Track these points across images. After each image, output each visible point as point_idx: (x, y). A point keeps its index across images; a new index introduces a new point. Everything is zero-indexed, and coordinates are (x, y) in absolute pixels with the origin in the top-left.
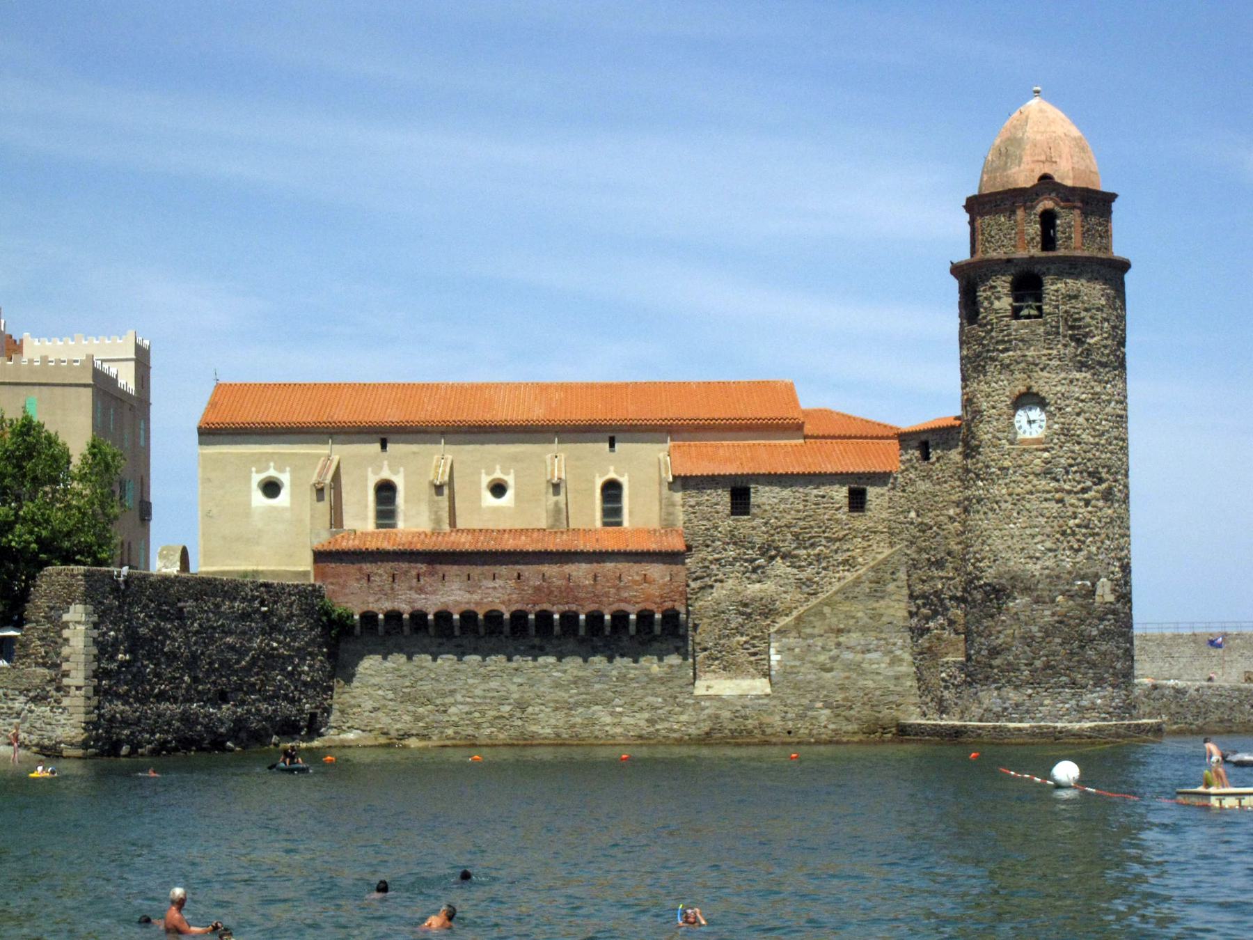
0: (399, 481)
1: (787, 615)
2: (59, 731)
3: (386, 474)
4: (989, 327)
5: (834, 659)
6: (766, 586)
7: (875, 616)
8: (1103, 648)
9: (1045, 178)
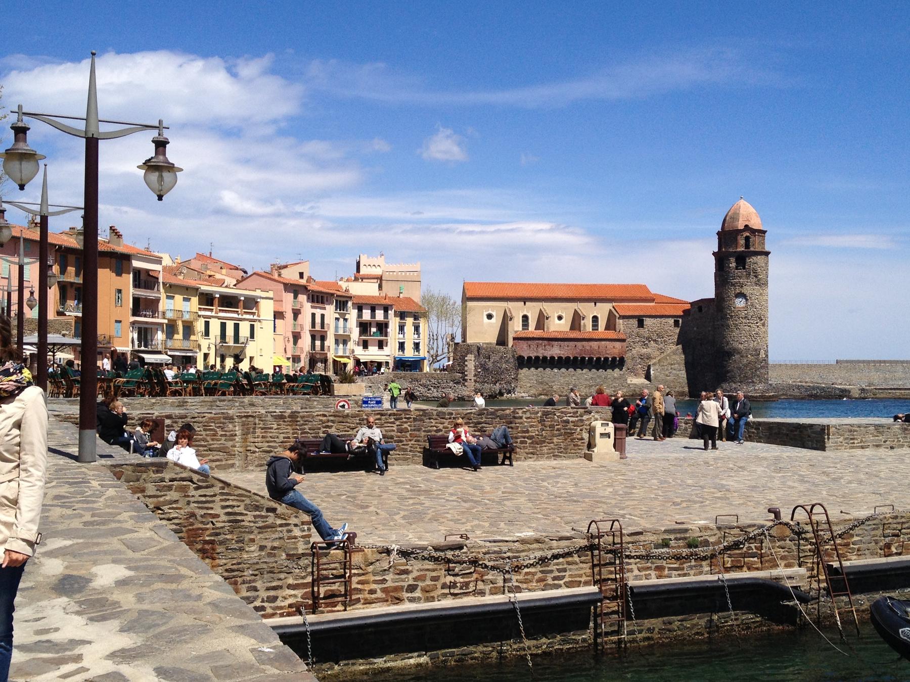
0: (529, 315)
2: (464, 392)
3: (525, 313)
5: (670, 373)
8: (762, 371)
9: (746, 226)
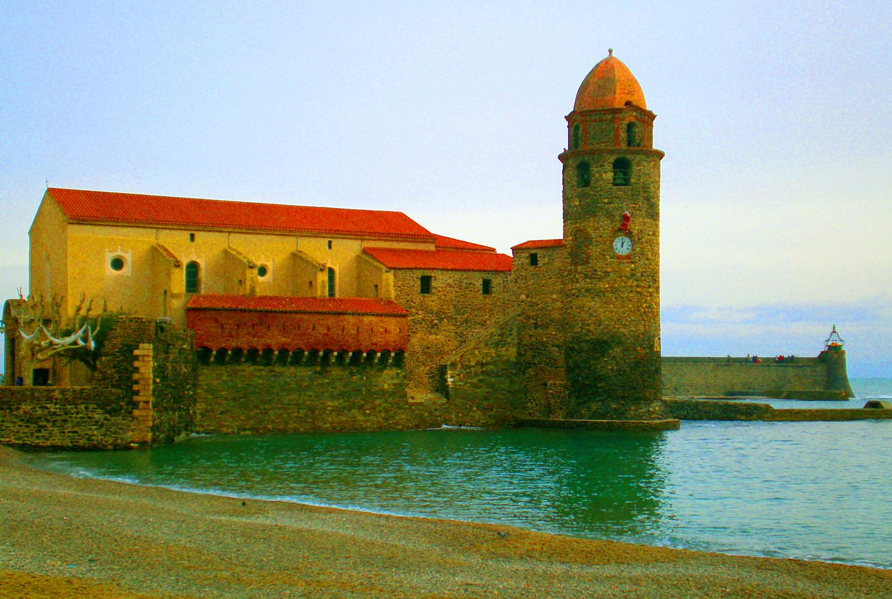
1: (449, 354)
4: (599, 189)
5: (480, 381)
6: (438, 337)
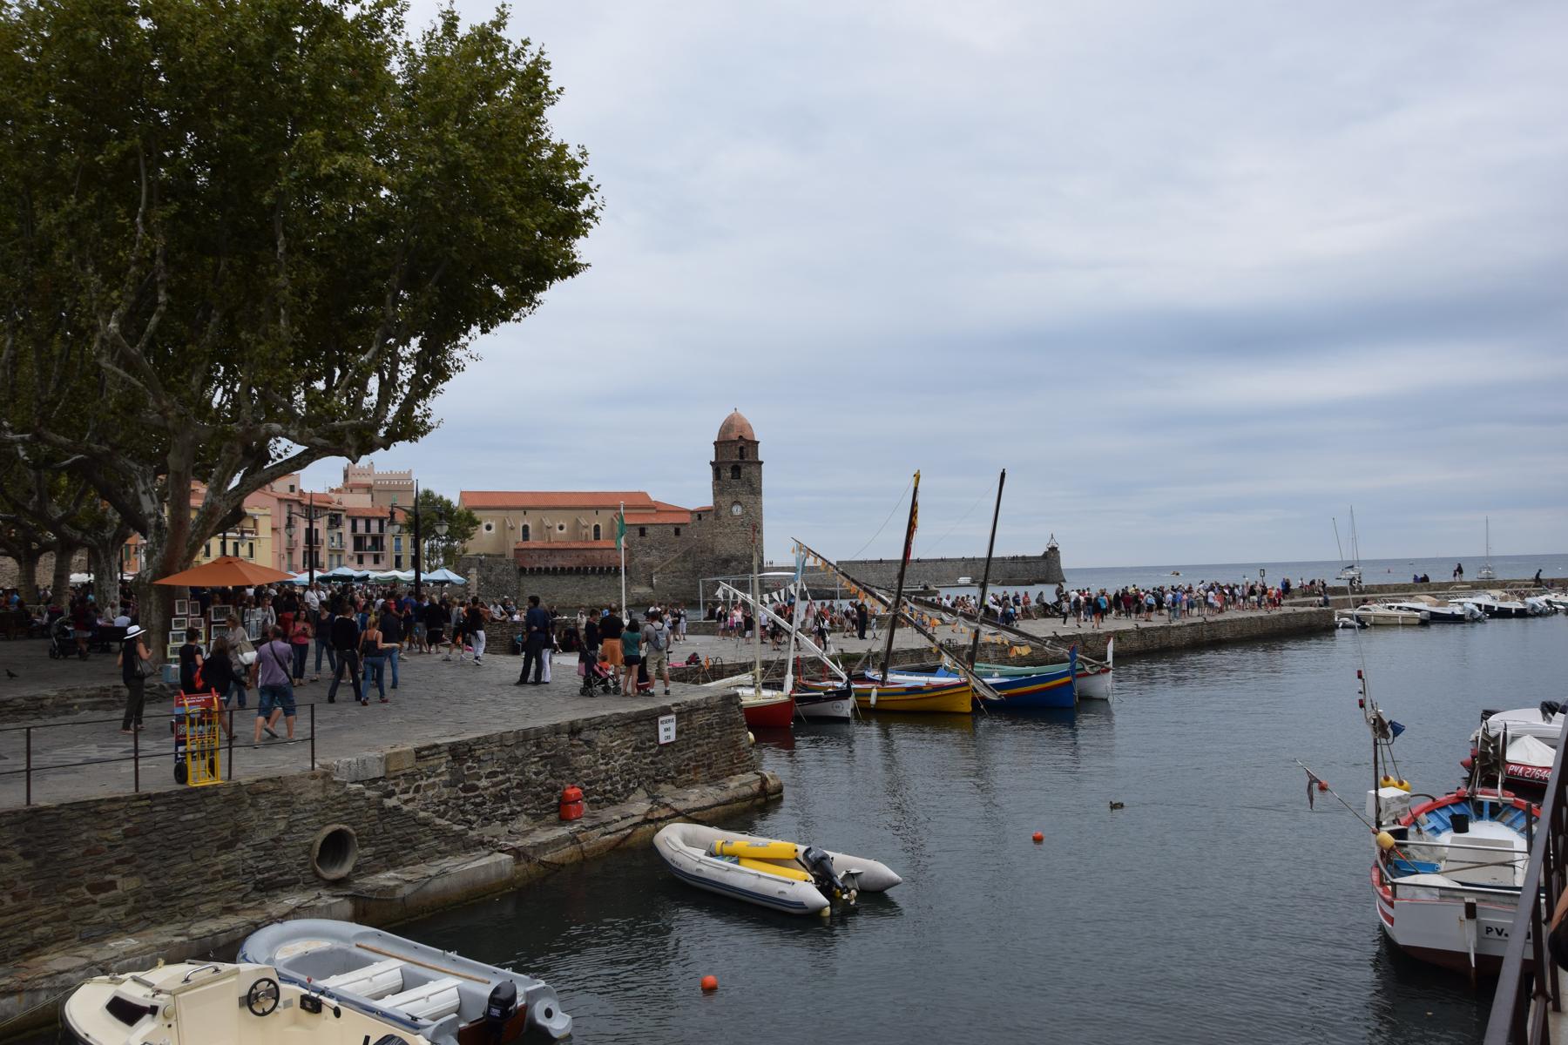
3: (526, 523)
7: (684, 567)
